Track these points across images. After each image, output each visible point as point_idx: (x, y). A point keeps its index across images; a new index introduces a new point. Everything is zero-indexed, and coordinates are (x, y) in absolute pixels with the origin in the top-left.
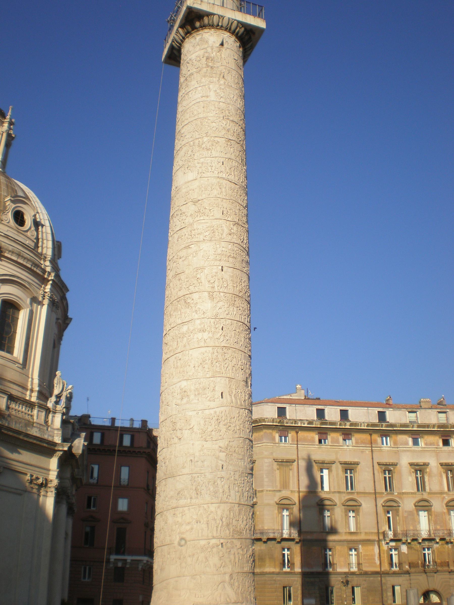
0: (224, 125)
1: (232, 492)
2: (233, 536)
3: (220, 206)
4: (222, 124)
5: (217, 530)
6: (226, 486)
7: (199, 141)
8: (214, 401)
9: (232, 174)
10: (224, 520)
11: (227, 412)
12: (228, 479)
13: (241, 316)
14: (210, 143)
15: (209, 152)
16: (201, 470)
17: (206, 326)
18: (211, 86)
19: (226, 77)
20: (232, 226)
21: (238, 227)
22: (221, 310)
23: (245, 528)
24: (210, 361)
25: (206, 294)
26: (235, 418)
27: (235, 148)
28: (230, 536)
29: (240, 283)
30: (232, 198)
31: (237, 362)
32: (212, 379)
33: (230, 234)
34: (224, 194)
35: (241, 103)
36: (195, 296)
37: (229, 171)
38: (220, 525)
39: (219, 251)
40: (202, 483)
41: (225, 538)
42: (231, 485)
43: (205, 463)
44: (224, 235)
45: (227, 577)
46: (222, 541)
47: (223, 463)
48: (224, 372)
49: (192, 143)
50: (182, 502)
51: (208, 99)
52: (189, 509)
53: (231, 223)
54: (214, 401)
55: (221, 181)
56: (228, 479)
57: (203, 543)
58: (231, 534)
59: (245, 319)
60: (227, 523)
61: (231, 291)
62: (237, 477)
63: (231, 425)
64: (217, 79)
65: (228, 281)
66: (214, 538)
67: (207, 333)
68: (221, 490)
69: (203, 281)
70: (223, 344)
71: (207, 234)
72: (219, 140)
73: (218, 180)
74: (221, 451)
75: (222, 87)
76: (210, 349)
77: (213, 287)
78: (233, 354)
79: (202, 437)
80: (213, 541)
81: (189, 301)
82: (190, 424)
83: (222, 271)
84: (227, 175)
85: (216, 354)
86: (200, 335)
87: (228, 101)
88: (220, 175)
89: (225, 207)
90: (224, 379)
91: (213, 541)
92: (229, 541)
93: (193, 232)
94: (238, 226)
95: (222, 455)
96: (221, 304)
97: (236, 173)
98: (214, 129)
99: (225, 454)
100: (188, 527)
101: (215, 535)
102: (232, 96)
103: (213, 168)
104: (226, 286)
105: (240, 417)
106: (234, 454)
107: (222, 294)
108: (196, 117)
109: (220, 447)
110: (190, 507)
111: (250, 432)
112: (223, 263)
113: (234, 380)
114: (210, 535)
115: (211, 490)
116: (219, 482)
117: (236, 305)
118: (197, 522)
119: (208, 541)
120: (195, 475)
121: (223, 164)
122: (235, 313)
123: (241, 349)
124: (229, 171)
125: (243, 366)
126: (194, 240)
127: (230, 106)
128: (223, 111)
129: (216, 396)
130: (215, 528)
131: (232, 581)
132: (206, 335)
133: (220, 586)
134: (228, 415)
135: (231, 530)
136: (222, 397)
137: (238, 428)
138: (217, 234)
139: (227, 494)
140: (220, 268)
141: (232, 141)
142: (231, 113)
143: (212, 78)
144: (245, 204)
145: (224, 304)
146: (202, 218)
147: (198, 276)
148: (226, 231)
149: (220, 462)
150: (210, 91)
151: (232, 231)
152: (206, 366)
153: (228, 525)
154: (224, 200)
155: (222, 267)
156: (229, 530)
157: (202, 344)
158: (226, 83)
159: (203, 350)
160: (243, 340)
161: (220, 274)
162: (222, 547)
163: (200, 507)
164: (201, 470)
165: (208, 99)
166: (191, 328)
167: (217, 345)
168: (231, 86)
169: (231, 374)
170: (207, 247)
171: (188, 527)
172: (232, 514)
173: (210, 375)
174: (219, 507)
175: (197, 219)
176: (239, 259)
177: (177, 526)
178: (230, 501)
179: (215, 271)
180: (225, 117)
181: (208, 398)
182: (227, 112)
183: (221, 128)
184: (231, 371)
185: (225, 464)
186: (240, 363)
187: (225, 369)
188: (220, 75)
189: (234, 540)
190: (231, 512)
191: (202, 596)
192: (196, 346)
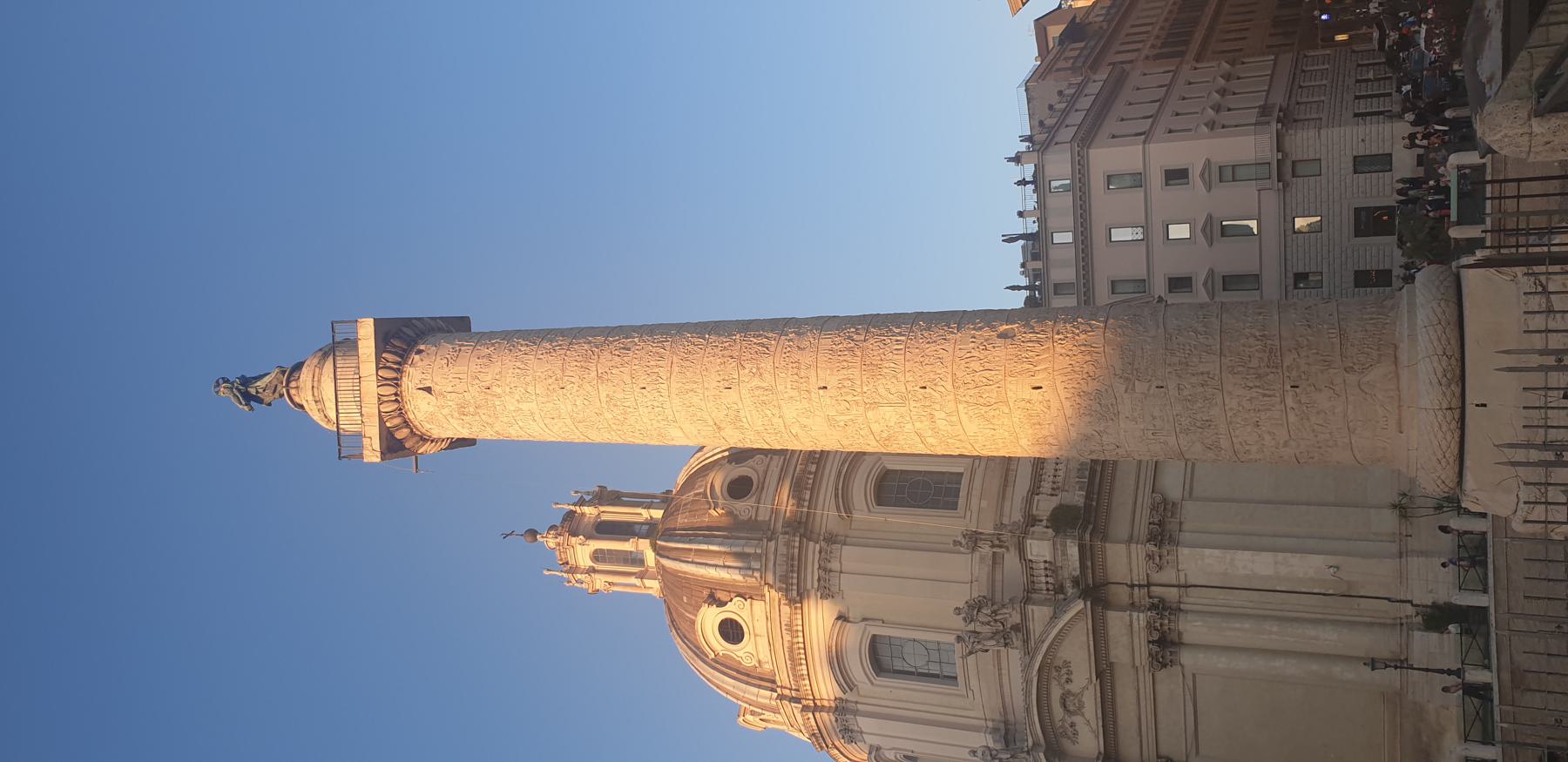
0: (576, 387)
1: (1202, 368)
2: (1277, 368)
3: (717, 392)
4: (575, 390)
5: (1269, 396)
6: (1194, 380)
7: (614, 424)
8: (1049, 401)
9: (657, 370)
10: (1251, 385)
11: (1065, 379)
12: (1180, 377)
13: (895, 352)
14: (615, 409)
15: (629, 410)
16: (1168, 421)
17: (924, 413)
18: (512, 408)
19: (487, 384)
20: (747, 371)
21: (745, 358)
22: (893, 391)
23: (1262, 341)
24: (981, 407)
25: (870, 414)
26: (1073, 363)
27: (610, 364)
28: (1278, 373)
29: (839, 353)
30: (698, 372)
31: (975, 359)
32: (1012, 405)
33: (761, 375)
34: (695, 386)
35: (523, 349)
36: (875, 427)
37: (654, 377)
38: (1260, 391)
39: (794, 393)
40: (1189, 419)
41: (1281, 382)
42: (1190, 371)
43: (1156, 414)
44: (764, 385)
45: (1352, 378)
46: (1288, 387)
47: (1154, 387)
48: (997, 385)
49: (619, 432)
50: (1224, 443)
51: (537, 412)
52: (1237, 437)
53: (741, 372)
54: (1049, 401)
55: (673, 390)
56: (1180, 377)
57: (1292, 418)
58: (1274, 370)
59: (897, 341)
60: (1256, 378)
61: (857, 372)
62: (1175, 360)
63: (1086, 371)
64: (495, 398)
65: (841, 377)
66: (1283, 401)
67: (935, 413)
68: (1200, 389)
69: (849, 417)
70: (950, 387)
71: (768, 412)
72: (605, 395)
73: (674, 396)
74: (1133, 389)
75: (508, 390)
76: (961, 407)
77: (857, 403)
78: (962, 367)
79: (1112, 420)
80: (1290, 402)
81: (885, 435)
82: (1092, 435)
83: (825, 388)
84: (661, 381)
85: (968, 398)
86: (941, 424)
87: (528, 379)
88: (665, 393)
89: (718, 384)
90: (1009, 386)
91: (1290, 402)
92: (1287, 374)
93: (769, 431)
94: (743, 358)
95: (1140, 387)
96: (882, 390)
97: (652, 363)
98: (586, 402)
99: (1137, 382)
100: (1267, 437)
101: (1278, 400)
102: (518, 371)
103: (656, 404)
104: (850, 383)
105: (1070, 353)
106: (1136, 366)
107: (865, 389)
108: (573, 427)
109: (1126, 391)
110: (1233, 434)
111: (1090, 325)
112: (813, 387)
113: (1007, 365)
114: (1278, 407)
115: (1201, 406)
116: (1186, 393)
117: (880, 362)
118: (1258, 426)
119: (1288, 410)
120: (1178, 429)
121: (644, 388)
122: (893, 365)
123: (951, 350)
124: (654, 377)
125: (981, 347)
126: (783, 430)
127: (537, 374)
128: (551, 388)
129: (1041, 398)
130: (1265, 399)
131: (1356, 367)
132: (939, 415)
133: (1367, 391)
134: (1070, 377)
135: (1269, 370)
136: (1041, 388)
137: (1088, 358)
138: (765, 398)
139: (1206, 379)
140: (821, 391)
141: (600, 372)
142: (550, 373)
143: (498, 407)
144: (701, 340)
145: (881, 386)
146: (744, 420)
147: (842, 424)
148: (756, 382)
149: (1152, 392)
150: (521, 409)
151: (754, 370)
152: (992, 413)
153: (1259, 377)
154: (706, 385)
155: (820, 388)
156: (1268, 375)
157: (954, 419)
158: (498, 383)
159: (964, 418)
160: (933, 347)
161: (832, 392)
162: (1297, 387)
163: (1231, 423)
164: (1168, 421)
165: (537, 412)
166: (930, 433)
167: (951, 397)
168: (500, 372)
169: (997, 372)
170: (790, 412)
171: (1267, 437)
172: (1240, 369)
173: (1005, 407)
174: (1230, 393)
175: (746, 426)
176: (797, 355)
177: (1265, 450)
178: (1218, 372)
179: (828, 400)
180: (562, 386)
181: (1045, 410)
182: (550, 381)
183: (581, 391)
184: (993, 373)
185: (1155, 384)
186: (975, 353)
187: (991, 383)
188: (485, 393)
189: (1285, 365)
190: (1235, 371)
191: (1385, 419)
192: (959, 426)
